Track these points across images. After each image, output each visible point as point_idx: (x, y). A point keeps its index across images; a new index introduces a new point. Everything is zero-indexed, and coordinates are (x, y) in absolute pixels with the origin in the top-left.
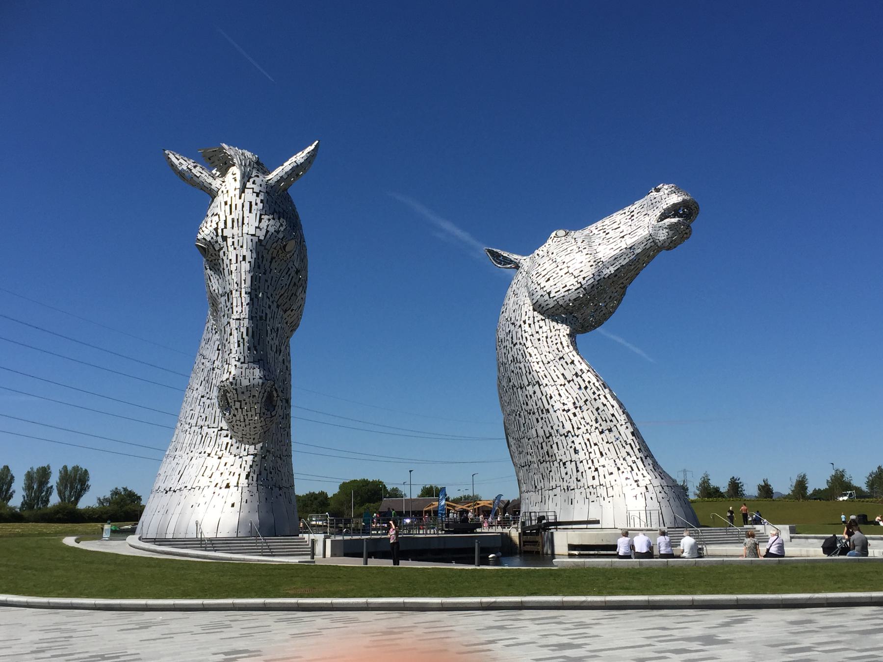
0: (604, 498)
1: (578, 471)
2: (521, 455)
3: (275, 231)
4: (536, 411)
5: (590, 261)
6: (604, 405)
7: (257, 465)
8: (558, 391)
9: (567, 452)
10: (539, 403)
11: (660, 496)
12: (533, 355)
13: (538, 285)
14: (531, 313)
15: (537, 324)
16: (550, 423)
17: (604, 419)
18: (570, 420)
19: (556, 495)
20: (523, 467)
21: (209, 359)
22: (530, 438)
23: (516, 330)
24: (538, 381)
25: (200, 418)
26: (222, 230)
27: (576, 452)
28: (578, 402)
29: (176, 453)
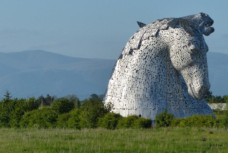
1: (186, 103)
21: (154, 71)
27: (185, 98)
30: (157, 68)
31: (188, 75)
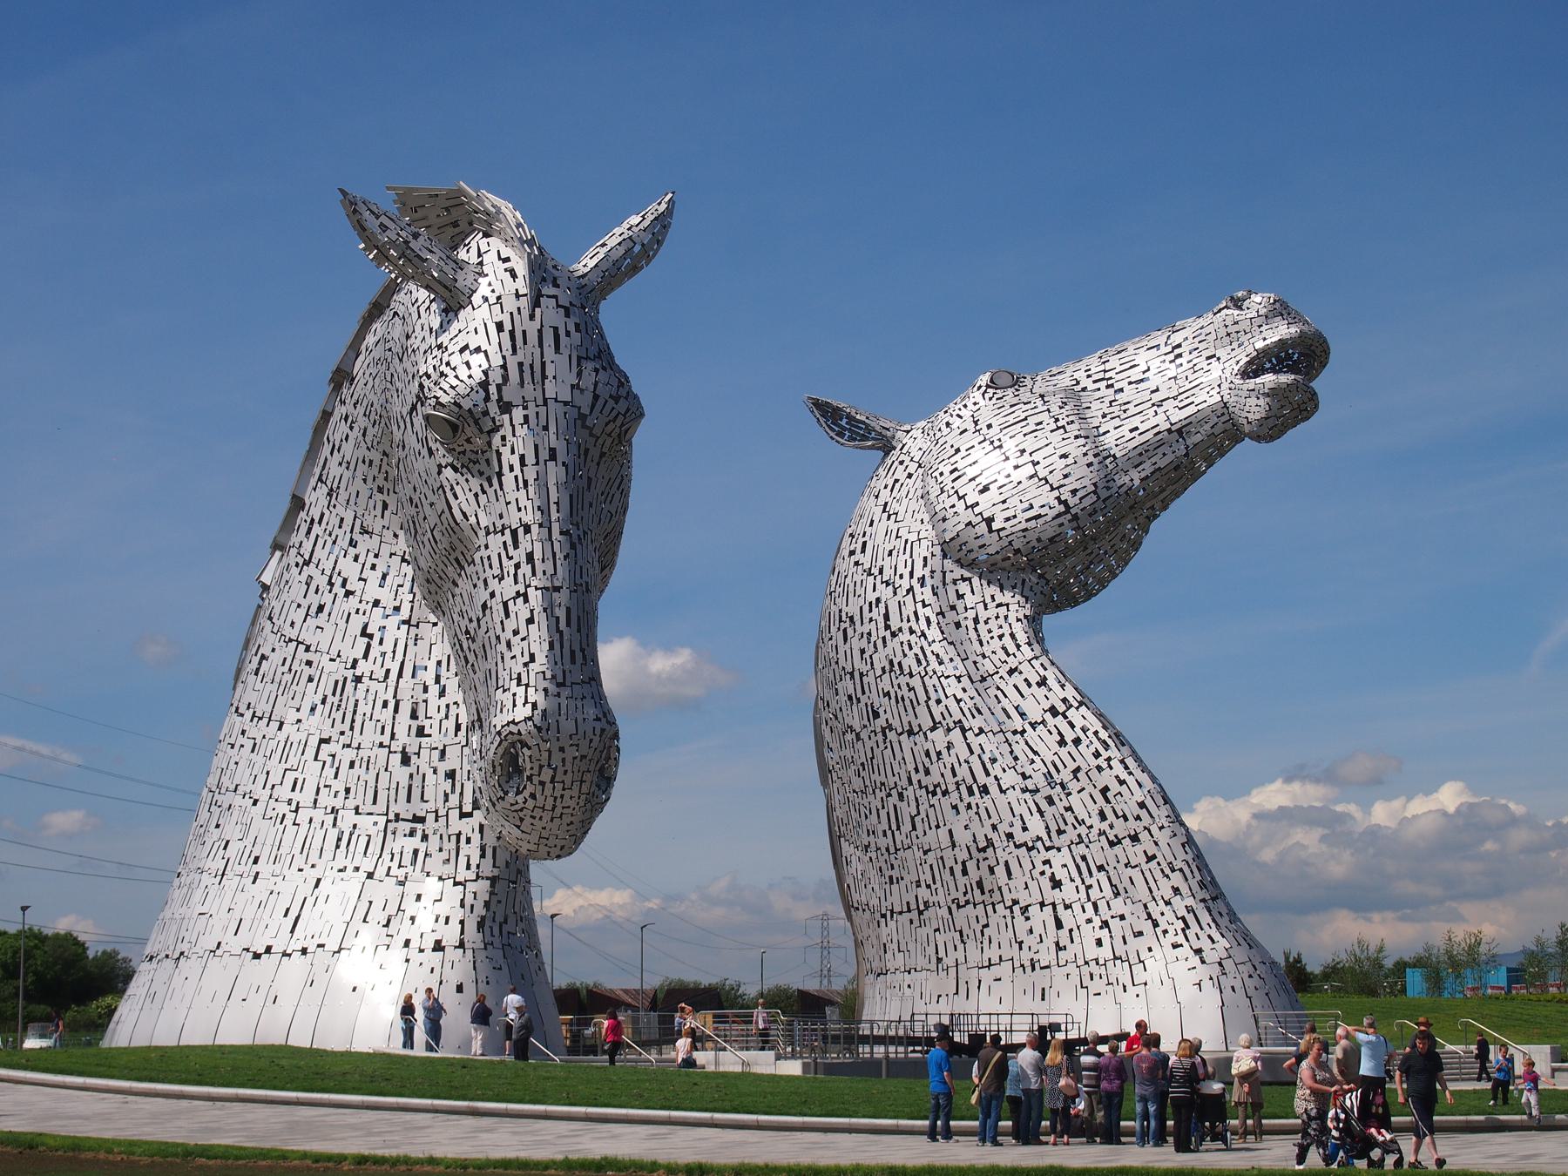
0: (1124, 987)
1: (1059, 925)
2: (895, 887)
3: (611, 396)
4: (952, 788)
5: (1085, 454)
6: (1122, 782)
7: (499, 902)
8: (1010, 745)
9: (1033, 885)
10: (963, 772)
11: (1250, 983)
12: (946, 659)
13: (960, 498)
14: (935, 563)
15: (951, 589)
16: (990, 817)
17: (1120, 814)
18: (1041, 813)
19: (1000, 979)
20: (901, 913)
21: (334, 654)
22: (930, 850)
23: (899, 597)
24: (960, 721)
25: (324, 791)
26: (499, 387)
27: (1056, 884)
28: (1058, 771)
29: (256, 868)
30: (357, 623)
31: (458, 646)
